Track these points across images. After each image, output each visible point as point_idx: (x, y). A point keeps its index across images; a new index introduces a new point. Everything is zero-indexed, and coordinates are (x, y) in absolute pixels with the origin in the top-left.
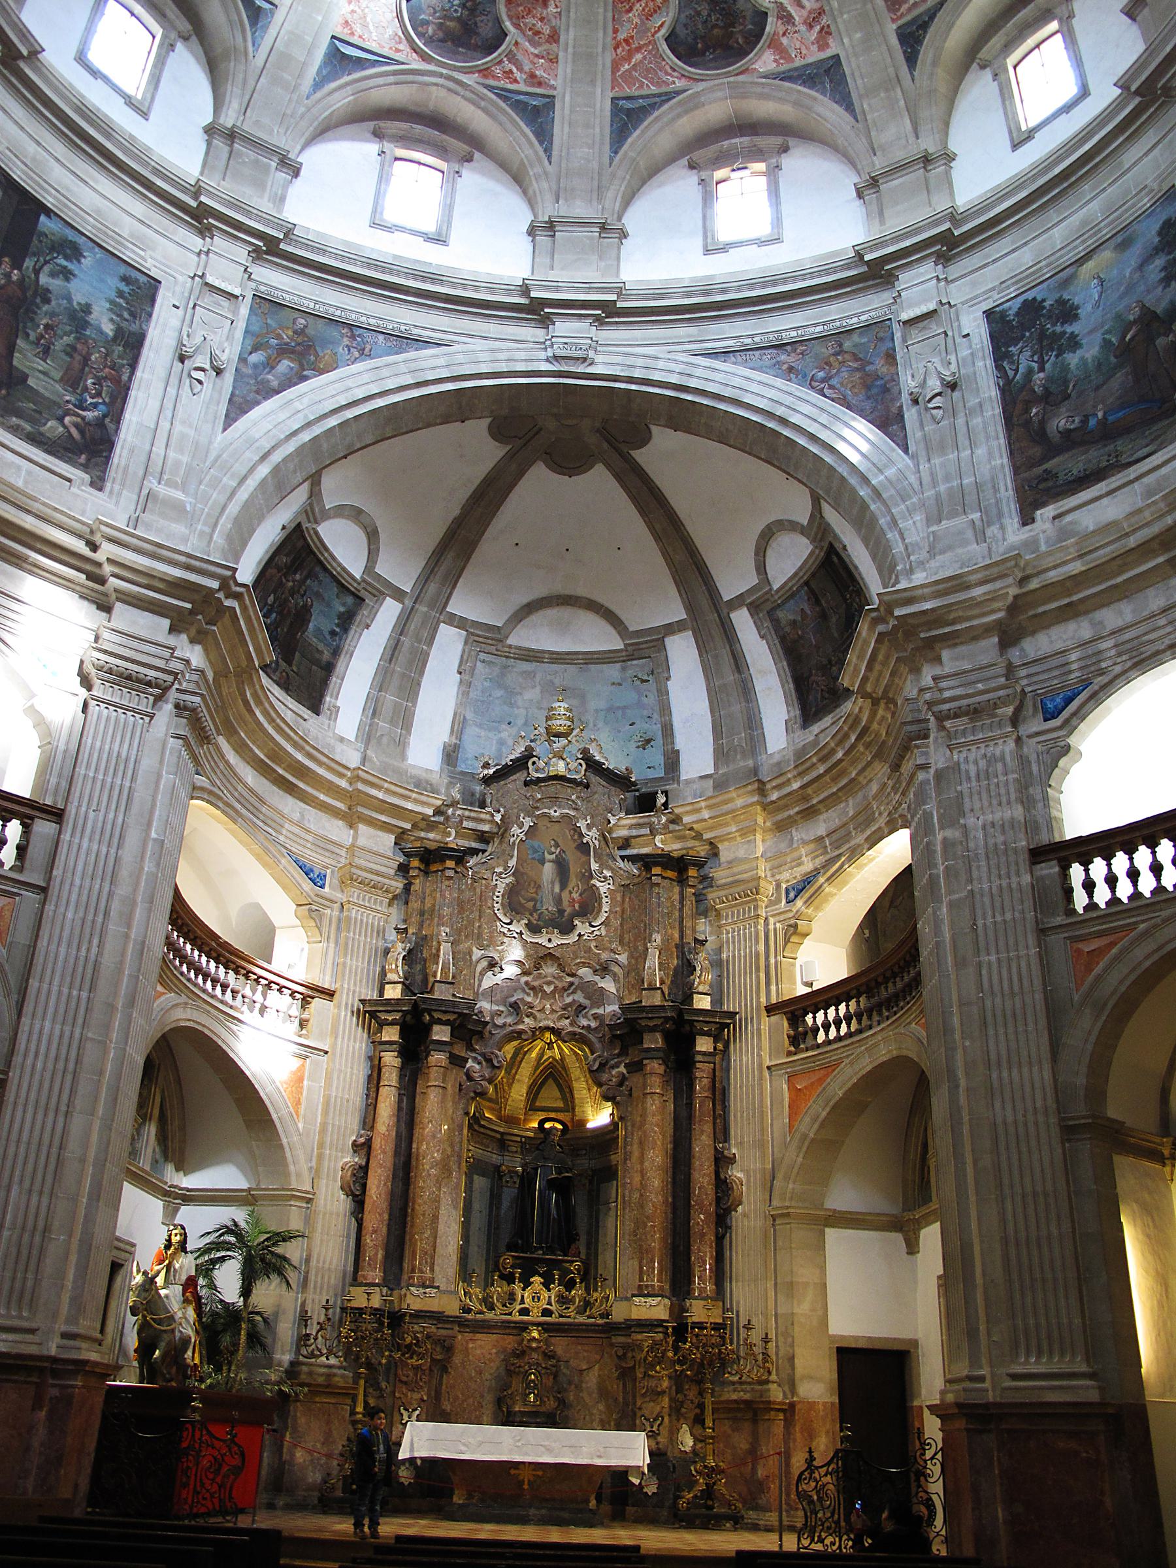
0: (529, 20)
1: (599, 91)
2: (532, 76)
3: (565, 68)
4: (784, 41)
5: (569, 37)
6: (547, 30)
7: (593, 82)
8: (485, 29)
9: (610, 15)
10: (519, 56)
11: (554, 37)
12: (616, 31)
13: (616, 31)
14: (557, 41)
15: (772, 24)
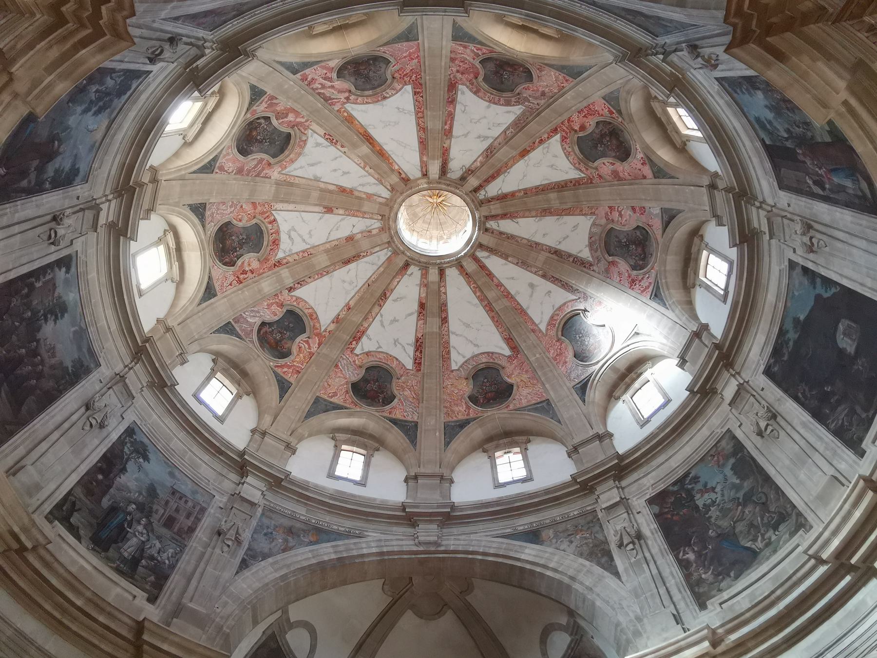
0: (466, 66)
1: (426, 45)
2: (465, 47)
3: (446, 52)
4: (325, 71)
5: (445, 61)
6: (457, 62)
7: (429, 48)
8: (491, 66)
9: (423, 68)
10: (472, 55)
11: (453, 60)
12: (419, 62)
13: (419, 62)
14: (451, 58)
15: (334, 75)
